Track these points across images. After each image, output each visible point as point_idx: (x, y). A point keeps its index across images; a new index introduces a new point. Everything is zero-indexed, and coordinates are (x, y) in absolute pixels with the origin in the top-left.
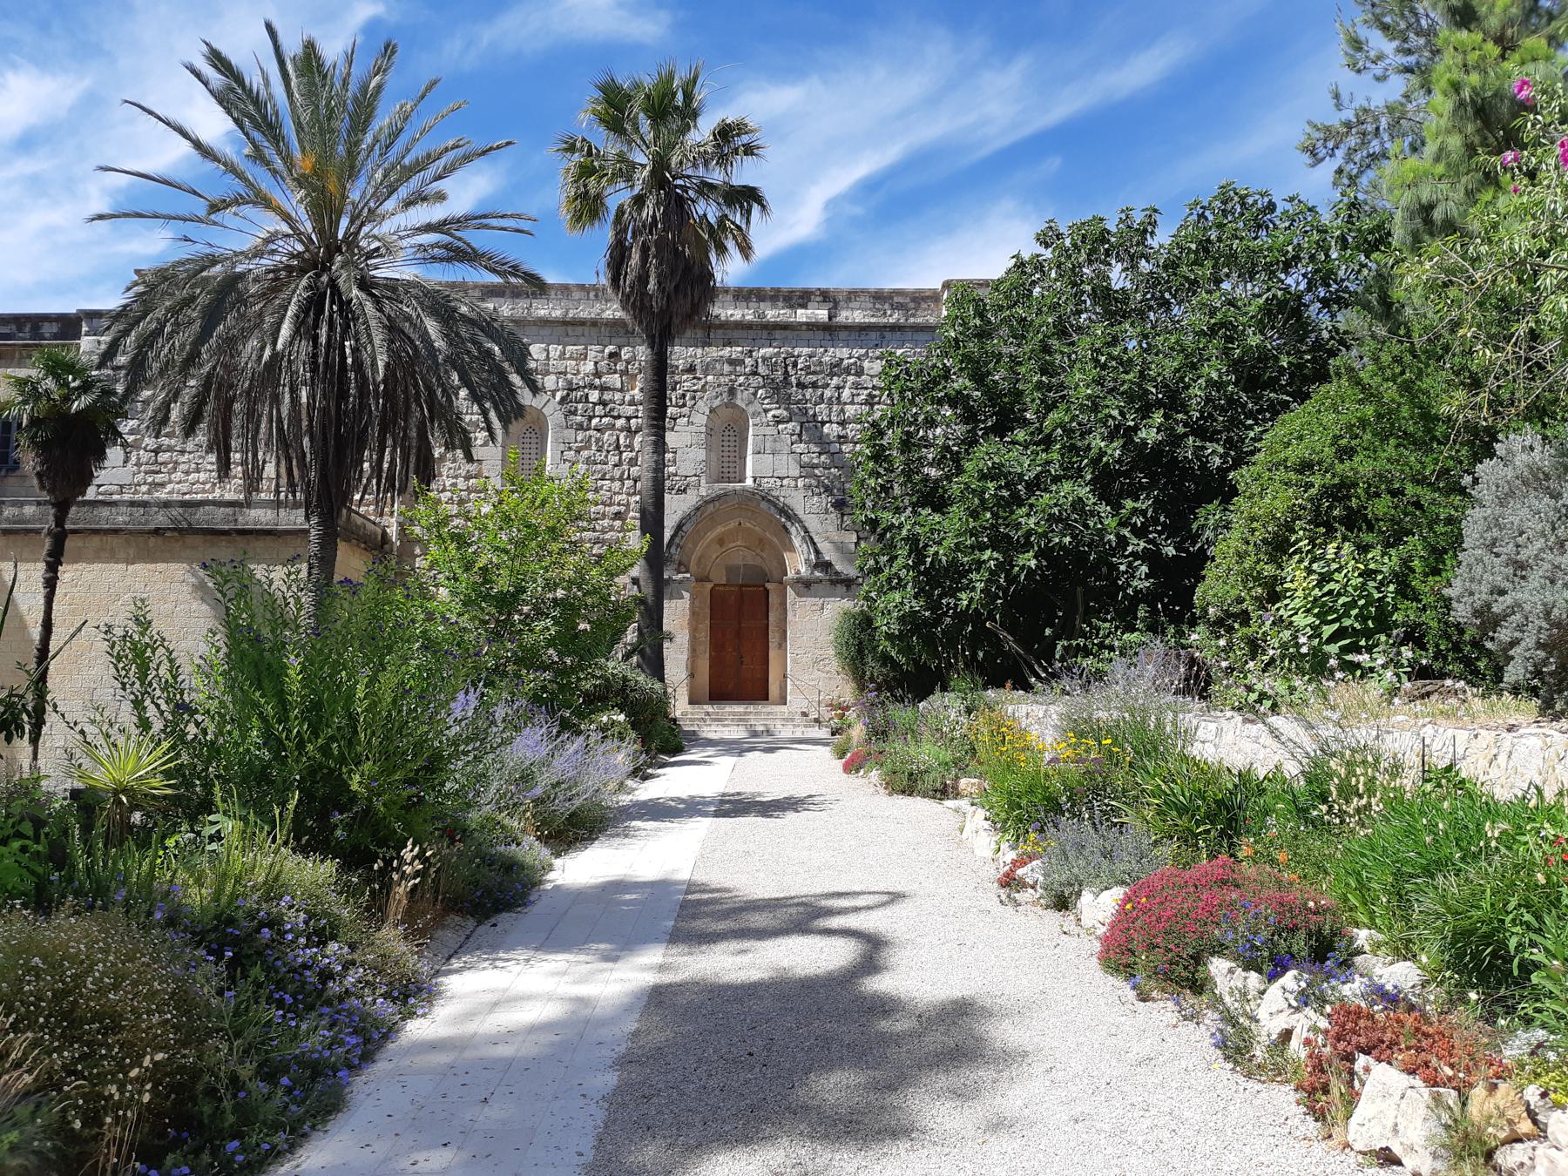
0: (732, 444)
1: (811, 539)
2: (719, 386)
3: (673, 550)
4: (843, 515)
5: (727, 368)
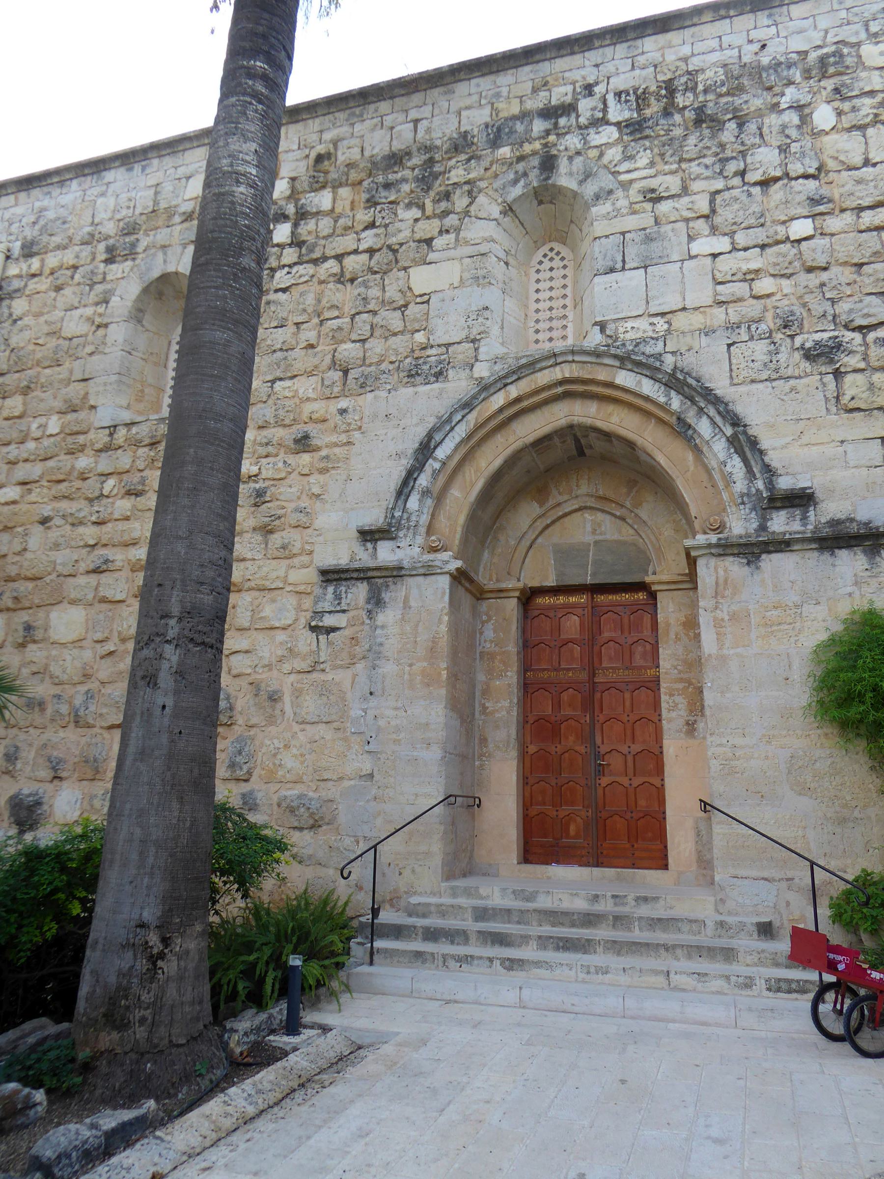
2: (521, 159)
3: (413, 503)
4: (838, 374)
5: (539, 126)
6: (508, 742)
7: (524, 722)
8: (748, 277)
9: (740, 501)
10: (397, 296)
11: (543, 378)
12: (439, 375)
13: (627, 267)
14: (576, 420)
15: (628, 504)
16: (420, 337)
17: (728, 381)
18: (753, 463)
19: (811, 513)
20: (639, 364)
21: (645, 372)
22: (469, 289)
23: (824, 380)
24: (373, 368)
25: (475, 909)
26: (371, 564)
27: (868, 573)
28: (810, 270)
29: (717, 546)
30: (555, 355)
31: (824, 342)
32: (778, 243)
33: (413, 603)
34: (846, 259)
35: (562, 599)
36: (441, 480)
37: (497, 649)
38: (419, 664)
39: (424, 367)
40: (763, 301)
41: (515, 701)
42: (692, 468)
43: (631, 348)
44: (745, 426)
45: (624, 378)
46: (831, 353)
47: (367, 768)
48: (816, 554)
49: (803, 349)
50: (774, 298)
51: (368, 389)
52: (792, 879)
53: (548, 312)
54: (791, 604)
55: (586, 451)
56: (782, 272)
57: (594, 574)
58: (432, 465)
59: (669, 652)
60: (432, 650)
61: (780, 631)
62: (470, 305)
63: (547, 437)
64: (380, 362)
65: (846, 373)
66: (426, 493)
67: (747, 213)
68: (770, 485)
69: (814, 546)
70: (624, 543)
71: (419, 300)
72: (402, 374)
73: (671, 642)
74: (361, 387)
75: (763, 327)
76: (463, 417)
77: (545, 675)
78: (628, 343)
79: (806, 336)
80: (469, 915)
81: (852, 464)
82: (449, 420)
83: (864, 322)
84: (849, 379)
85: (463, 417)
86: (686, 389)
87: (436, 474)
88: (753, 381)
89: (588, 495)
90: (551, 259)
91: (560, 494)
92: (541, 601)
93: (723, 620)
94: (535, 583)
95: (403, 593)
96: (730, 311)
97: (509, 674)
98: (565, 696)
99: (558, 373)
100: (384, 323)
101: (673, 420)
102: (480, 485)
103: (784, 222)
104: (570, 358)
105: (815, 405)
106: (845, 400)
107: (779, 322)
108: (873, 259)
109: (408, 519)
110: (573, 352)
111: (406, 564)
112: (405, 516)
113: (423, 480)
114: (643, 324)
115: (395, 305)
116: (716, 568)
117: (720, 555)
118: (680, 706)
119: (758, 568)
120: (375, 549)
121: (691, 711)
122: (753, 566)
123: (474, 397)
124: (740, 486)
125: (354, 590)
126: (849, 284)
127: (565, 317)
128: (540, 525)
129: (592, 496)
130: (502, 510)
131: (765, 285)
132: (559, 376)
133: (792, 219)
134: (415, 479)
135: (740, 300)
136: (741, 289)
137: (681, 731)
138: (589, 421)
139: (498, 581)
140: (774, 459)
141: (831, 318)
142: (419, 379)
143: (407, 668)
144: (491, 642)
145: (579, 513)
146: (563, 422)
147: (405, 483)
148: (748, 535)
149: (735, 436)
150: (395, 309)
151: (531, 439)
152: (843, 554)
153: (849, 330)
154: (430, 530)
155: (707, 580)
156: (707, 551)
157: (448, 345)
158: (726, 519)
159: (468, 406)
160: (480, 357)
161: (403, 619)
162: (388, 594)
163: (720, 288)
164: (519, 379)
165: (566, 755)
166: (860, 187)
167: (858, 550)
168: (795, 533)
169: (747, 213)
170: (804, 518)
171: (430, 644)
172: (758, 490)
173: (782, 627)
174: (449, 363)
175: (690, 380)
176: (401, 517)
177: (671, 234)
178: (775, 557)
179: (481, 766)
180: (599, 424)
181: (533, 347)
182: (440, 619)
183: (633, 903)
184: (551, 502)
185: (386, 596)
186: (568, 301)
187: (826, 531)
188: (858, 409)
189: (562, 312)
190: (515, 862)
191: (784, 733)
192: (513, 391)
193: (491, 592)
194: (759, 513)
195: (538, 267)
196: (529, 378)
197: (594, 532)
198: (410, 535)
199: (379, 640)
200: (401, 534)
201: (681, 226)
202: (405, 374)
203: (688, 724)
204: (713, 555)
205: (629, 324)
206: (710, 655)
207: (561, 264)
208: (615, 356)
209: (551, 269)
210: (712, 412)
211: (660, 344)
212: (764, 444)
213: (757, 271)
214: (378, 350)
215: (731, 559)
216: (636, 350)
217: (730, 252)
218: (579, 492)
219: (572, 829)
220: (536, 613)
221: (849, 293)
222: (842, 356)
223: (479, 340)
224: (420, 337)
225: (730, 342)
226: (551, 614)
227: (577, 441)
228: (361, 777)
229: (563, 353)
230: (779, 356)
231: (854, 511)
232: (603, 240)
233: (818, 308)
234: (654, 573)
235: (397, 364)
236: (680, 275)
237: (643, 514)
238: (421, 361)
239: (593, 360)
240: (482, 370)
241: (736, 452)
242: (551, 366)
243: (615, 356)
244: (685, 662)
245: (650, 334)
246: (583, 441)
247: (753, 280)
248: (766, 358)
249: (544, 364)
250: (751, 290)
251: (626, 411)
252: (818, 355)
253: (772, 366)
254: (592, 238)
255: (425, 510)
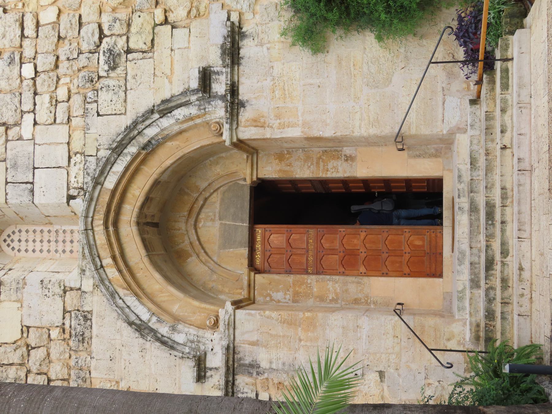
0: (31, 236)
1: (163, 102)
3: (180, 338)
4: (129, 51)
6: (358, 283)
7: (343, 274)
8: (54, 103)
9: (203, 111)
10: (19, 352)
11: (101, 238)
12: (86, 318)
13: (31, 181)
14: (134, 219)
15: (195, 195)
16: (55, 334)
17: (123, 116)
18: (179, 102)
19: (215, 69)
20: (102, 172)
21: (108, 169)
22: (24, 295)
23: (131, 59)
24: (72, 372)
25: (471, 288)
26: (223, 371)
27: (256, 38)
28: (57, 67)
29: (231, 124)
30: (86, 230)
31: (106, 59)
32: (35, 84)
33: (255, 338)
34: (54, 45)
35: (258, 246)
36: (165, 317)
37: (291, 290)
38: (300, 334)
39: (78, 330)
40: (72, 95)
41: (328, 277)
42: (178, 143)
43: (90, 178)
44: (154, 106)
45: (110, 183)
46: (114, 55)
47: (376, 376)
48: (241, 68)
49: (108, 70)
50: (72, 88)
51: (88, 375)
52: (443, 88)
53: (51, 244)
54: (272, 83)
55: (155, 221)
56: (55, 82)
57: (242, 221)
58: (153, 324)
59: (299, 170)
60: (290, 323)
61: (288, 90)
62: (37, 294)
63: (144, 241)
64: (69, 368)
65: (128, 47)
66: (173, 329)
67: (10, 103)
68: (195, 92)
69: (236, 68)
70: (222, 200)
71: (25, 335)
72: (81, 348)
73: (292, 169)
74: (85, 381)
75: (90, 94)
76: (120, 298)
77: (311, 259)
78: (86, 180)
79: (100, 69)
80: (475, 291)
81: (186, 45)
82: (121, 309)
83: (97, 36)
84: (132, 45)
85: (120, 298)
86: (124, 142)
87: (160, 321)
88: (125, 101)
89: (187, 222)
90: (12, 241)
91: (183, 242)
92: (258, 261)
93: (280, 124)
94: (246, 262)
95: (247, 346)
96: (75, 115)
97: (309, 281)
98: (326, 245)
99: (99, 228)
100: (38, 364)
101: (144, 152)
102: (172, 290)
103: (21, 81)
104: (90, 219)
105: (146, 65)
106: (145, 48)
107: (88, 85)
108: (57, 30)
109: (192, 342)
110: (86, 217)
111: (225, 343)
112: (189, 344)
113: (164, 330)
114: (74, 170)
115: (25, 354)
116: (245, 127)
117: (237, 124)
118: (335, 165)
119: (247, 101)
120: (211, 369)
121: (338, 158)
122: (246, 104)
123: (107, 289)
124: (193, 110)
125: (241, 387)
126: (70, 44)
127: (57, 231)
128: (203, 257)
129: (187, 220)
130: (191, 284)
131: (62, 93)
132: (102, 227)
133: (21, 76)
134: (162, 336)
135: (69, 108)
136: (62, 108)
137: (351, 165)
138: (136, 210)
139: (242, 288)
140: (177, 89)
141: (91, 55)
142: (87, 334)
143: (303, 343)
144: (285, 294)
145: (199, 230)
146: (134, 229)
147: (164, 343)
148: (226, 107)
149: (160, 112)
150: (29, 355)
151: (143, 252)
152: (242, 52)
153: (100, 45)
154: (201, 327)
155: (253, 132)
156: (234, 131)
157: (65, 311)
158: (214, 121)
159: (113, 295)
160: (78, 286)
161: (266, 347)
162: (246, 358)
163: (58, 121)
164: (99, 257)
165: (367, 245)
166: (7, 35)
167: (241, 44)
168: (227, 78)
169: (10, 103)
170: (218, 73)
171: (285, 325)
172: (197, 100)
173: (286, 88)
174: (78, 310)
175: (119, 139)
176: (190, 347)
177: (14, 151)
178: (241, 91)
179: (374, 303)
180: (139, 204)
181: (77, 247)
182: (268, 318)
183: (462, 185)
184: (189, 248)
185: (247, 361)
186: (46, 229)
187: (228, 61)
188: (153, 40)
189: (53, 234)
190: (441, 280)
191: (352, 89)
192: (107, 261)
193: (249, 292)
194: (212, 99)
195: (16, 251)
196: (100, 250)
197: (213, 220)
198: (203, 341)
199: (280, 366)
200: (202, 348)
201: (9, 144)
202: (81, 345)
203: (347, 160)
204: (237, 128)
205: (72, 179)
206: (302, 132)
207: (17, 234)
208: (94, 188)
209: (20, 241)
210: (141, 127)
211: (90, 159)
212: (167, 96)
213: (51, 97)
214: (58, 368)
215: (240, 117)
216: (91, 175)
217: (35, 114)
218: (184, 228)
219: (418, 243)
220: (266, 264)
221: (76, 44)
222: (116, 48)
223: (65, 287)
224: (55, 334)
225: (96, 114)
226: (268, 254)
227: (148, 224)
228: (381, 381)
229: (86, 224)
230: (111, 85)
231: (216, 45)
232: (8, 197)
233: (83, 60)
234: (245, 180)
235: (72, 353)
236: (44, 146)
237: (203, 185)
238: (73, 333)
239: (94, 203)
240: (88, 284)
241: (170, 112)
242: (93, 233)
243: (94, 188)
244: (305, 161)
245: (82, 166)
246: (149, 220)
247: (56, 101)
248: (111, 92)
249: (91, 238)
250: (63, 101)
251: (133, 185)
252: (114, 62)
253: (117, 89)
254: (5, 206)
255: (186, 330)
